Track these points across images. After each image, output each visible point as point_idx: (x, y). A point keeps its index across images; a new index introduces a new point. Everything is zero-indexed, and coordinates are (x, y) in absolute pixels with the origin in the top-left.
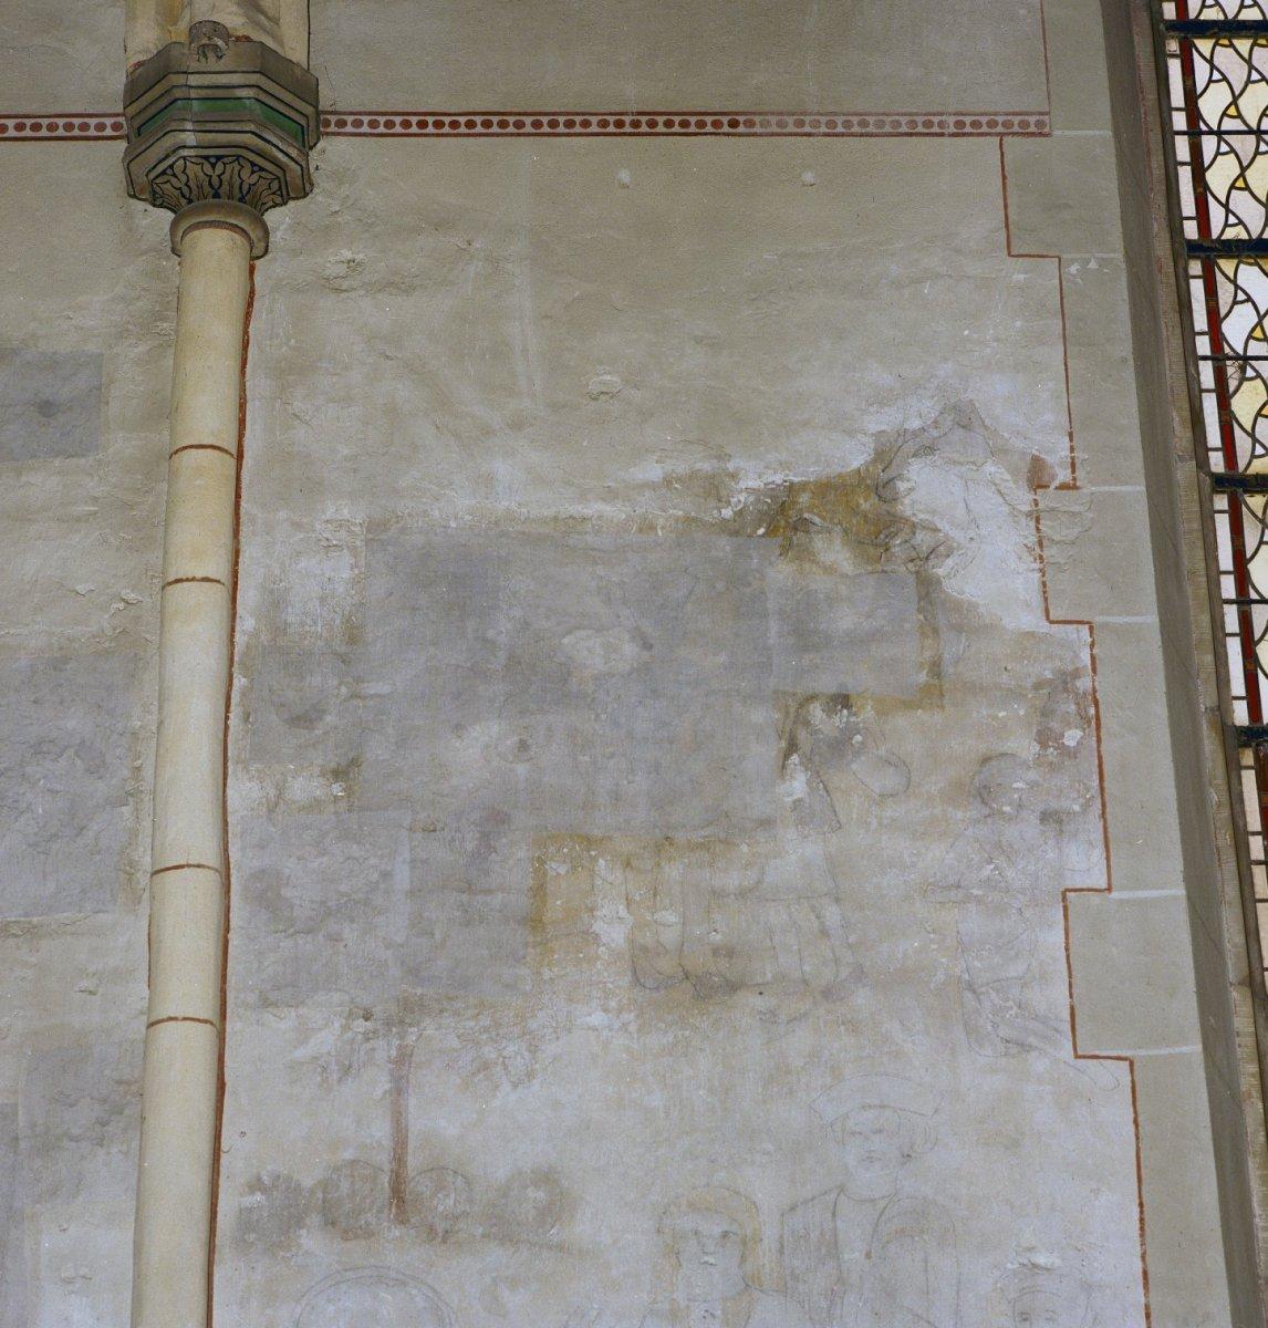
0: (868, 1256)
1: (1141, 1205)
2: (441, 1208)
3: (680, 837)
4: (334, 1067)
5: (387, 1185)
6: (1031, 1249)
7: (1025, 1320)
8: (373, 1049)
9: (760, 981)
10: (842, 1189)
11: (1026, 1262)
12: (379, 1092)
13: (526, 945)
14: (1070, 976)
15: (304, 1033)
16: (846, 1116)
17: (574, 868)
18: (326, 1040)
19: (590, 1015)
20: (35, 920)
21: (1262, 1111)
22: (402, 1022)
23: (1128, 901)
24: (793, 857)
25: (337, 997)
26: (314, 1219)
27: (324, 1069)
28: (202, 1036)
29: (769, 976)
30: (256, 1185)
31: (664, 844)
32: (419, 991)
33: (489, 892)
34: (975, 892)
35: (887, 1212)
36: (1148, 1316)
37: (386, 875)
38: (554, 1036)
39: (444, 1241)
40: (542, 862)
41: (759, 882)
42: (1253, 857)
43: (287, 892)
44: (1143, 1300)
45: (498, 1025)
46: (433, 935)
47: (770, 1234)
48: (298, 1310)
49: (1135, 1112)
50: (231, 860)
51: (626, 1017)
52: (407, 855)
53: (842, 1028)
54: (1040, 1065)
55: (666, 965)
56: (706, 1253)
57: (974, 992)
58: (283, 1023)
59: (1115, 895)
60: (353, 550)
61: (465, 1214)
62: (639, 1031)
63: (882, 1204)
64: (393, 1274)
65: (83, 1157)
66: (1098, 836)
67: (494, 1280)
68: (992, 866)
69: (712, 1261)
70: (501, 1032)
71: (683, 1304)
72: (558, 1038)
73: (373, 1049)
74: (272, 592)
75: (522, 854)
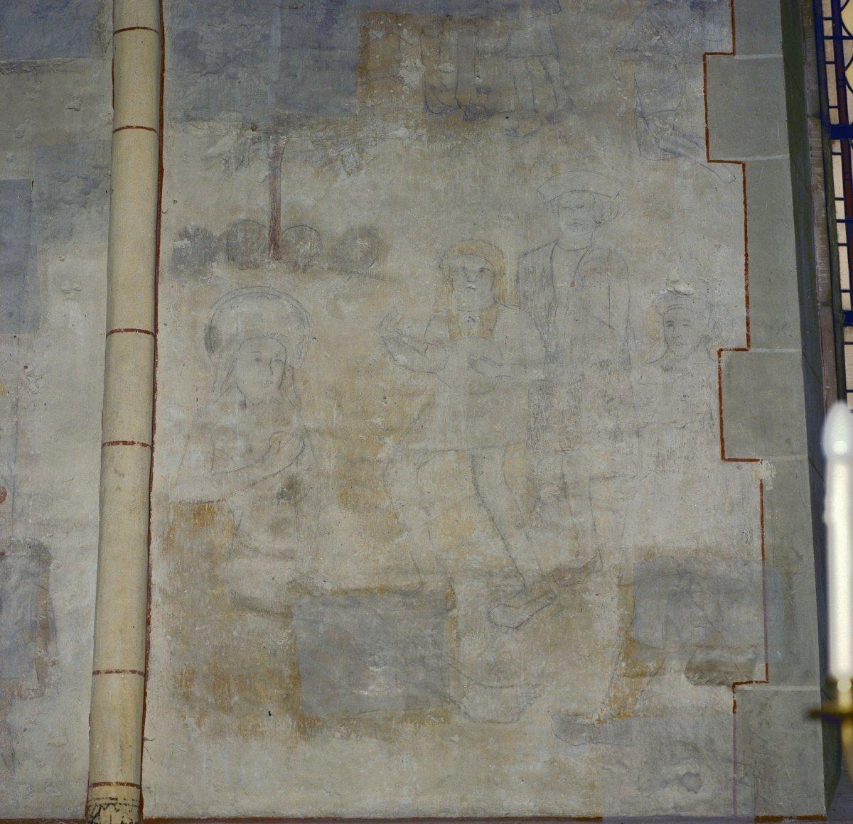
0: (573, 284)
1: (746, 255)
2: (302, 251)
3: (457, 15)
4: (233, 160)
5: (267, 236)
6: (675, 282)
7: (671, 325)
8: (258, 149)
9: (507, 110)
10: (557, 243)
11: (672, 289)
12: (262, 176)
13: (356, 84)
14: (706, 109)
16: (560, 197)
17: (388, 34)
19: (397, 130)
20: (38, 61)
21: (824, 197)
22: (276, 132)
23: (746, 61)
24: (530, 29)
25: (234, 115)
26: (221, 256)
28: (149, 138)
29: (512, 107)
30: (185, 234)
31: (445, 19)
33: (332, 49)
34: (647, 54)
35: (584, 258)
36: (748, 324)
37: (266, 37)
38: (374, 143)
39: (304, 271)
40: (366, 29)
41: (507, 45)
42: (826, 34)
43: (201, 47)
44: (745, 314)
45: (338, 135)
46: (296, 76)
47: (511, 270)
48: (212, 313)
49: (745, 196)
50: (165, 25)
51: (420, 131)
52: (279, 24)
53: (559, 140)
54: (685, 166)
55: (446, 98)
56: (469, 281)
57: (644, 118)
58: (199, 131)
59: (737, 57)
61: (318, 255)
62: (429, 140)
63: (582, 252)
64: (272, 292)
65: (73, 215)
66: (728, 19)
67: (335, 296)
68: (658, 37)
69: (474, 286)
70: (340, 139)
71: (455, 313)
72: (376, 144)
75: (353, 24)
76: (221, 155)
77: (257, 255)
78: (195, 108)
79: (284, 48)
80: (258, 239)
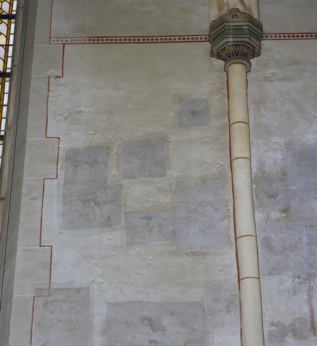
5: (310, 325)
15: (282, 283)
18: (288, 284)
22: (309, 279)
25: (290, 272)
26: (290, 334)
27: (289, 292)
30: (273, 324)
32: (313, 271)
43: (273, 243)
58: (276, 279)
60: (282, 150)
65: (223, 316)
73: (302, 287)
74: (260, 162)
76: (286, 289)
77: (306, 333)
78: (273, 270)
79: (308, 244)
80: (306, 326)
